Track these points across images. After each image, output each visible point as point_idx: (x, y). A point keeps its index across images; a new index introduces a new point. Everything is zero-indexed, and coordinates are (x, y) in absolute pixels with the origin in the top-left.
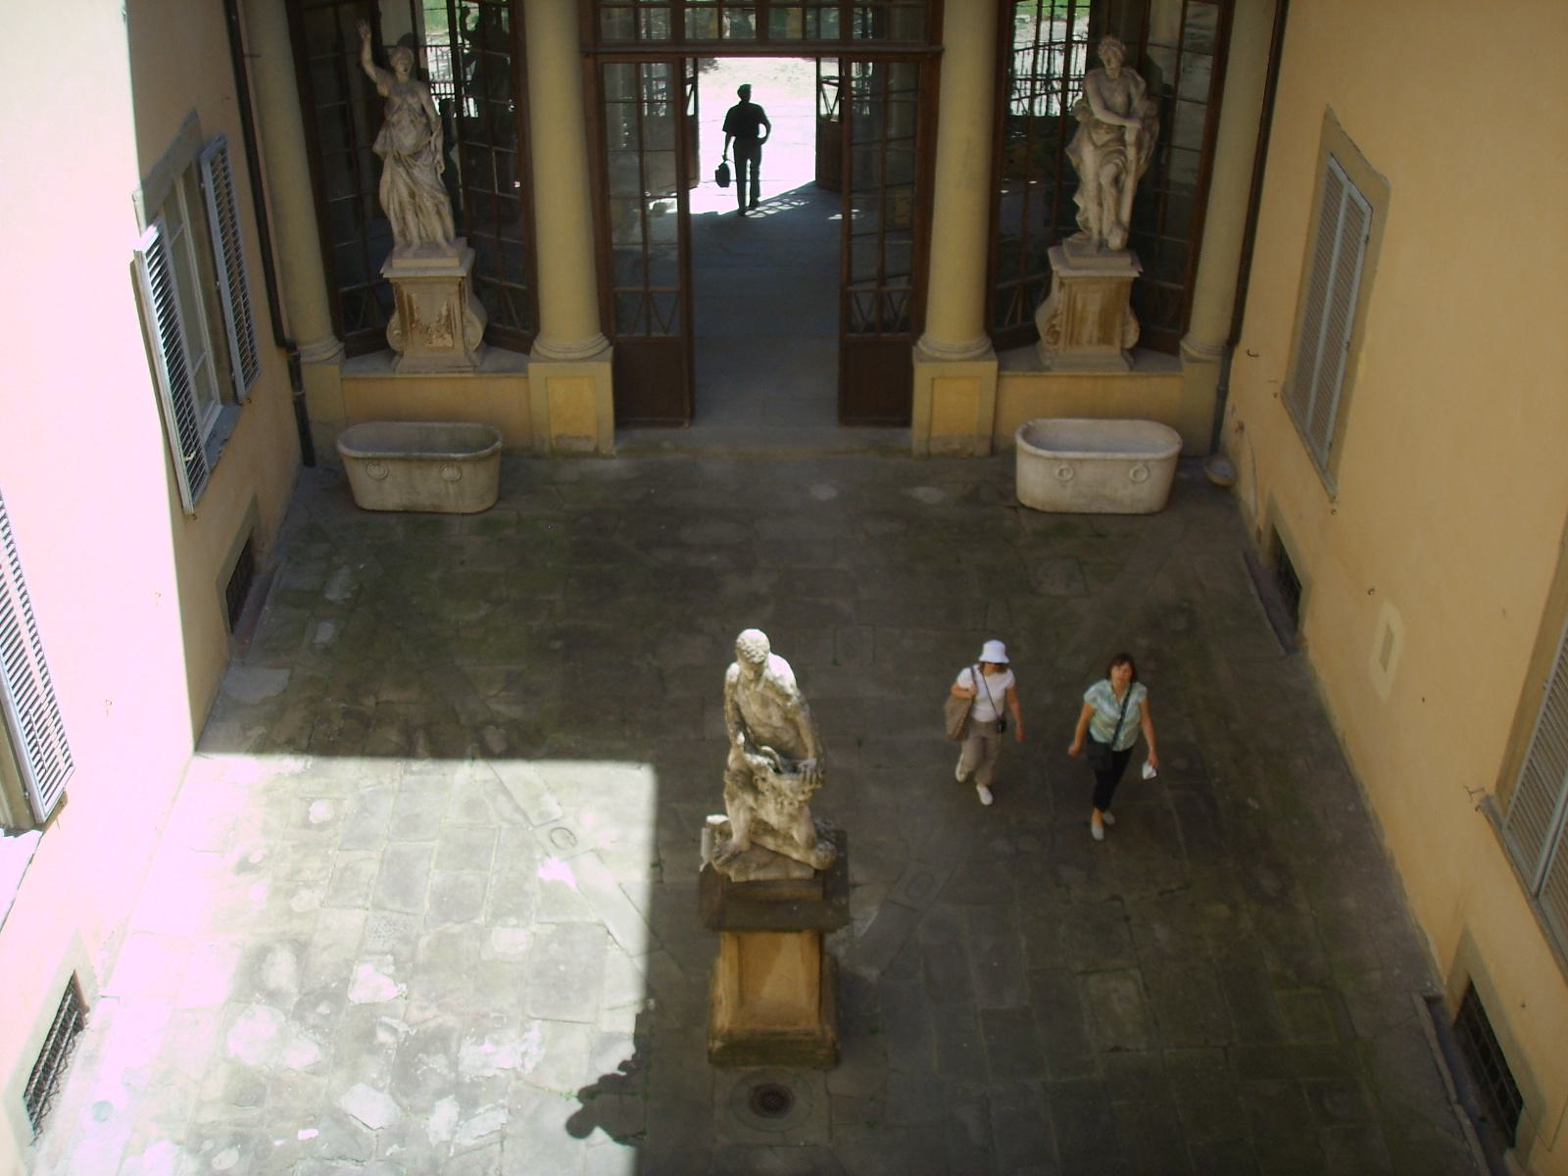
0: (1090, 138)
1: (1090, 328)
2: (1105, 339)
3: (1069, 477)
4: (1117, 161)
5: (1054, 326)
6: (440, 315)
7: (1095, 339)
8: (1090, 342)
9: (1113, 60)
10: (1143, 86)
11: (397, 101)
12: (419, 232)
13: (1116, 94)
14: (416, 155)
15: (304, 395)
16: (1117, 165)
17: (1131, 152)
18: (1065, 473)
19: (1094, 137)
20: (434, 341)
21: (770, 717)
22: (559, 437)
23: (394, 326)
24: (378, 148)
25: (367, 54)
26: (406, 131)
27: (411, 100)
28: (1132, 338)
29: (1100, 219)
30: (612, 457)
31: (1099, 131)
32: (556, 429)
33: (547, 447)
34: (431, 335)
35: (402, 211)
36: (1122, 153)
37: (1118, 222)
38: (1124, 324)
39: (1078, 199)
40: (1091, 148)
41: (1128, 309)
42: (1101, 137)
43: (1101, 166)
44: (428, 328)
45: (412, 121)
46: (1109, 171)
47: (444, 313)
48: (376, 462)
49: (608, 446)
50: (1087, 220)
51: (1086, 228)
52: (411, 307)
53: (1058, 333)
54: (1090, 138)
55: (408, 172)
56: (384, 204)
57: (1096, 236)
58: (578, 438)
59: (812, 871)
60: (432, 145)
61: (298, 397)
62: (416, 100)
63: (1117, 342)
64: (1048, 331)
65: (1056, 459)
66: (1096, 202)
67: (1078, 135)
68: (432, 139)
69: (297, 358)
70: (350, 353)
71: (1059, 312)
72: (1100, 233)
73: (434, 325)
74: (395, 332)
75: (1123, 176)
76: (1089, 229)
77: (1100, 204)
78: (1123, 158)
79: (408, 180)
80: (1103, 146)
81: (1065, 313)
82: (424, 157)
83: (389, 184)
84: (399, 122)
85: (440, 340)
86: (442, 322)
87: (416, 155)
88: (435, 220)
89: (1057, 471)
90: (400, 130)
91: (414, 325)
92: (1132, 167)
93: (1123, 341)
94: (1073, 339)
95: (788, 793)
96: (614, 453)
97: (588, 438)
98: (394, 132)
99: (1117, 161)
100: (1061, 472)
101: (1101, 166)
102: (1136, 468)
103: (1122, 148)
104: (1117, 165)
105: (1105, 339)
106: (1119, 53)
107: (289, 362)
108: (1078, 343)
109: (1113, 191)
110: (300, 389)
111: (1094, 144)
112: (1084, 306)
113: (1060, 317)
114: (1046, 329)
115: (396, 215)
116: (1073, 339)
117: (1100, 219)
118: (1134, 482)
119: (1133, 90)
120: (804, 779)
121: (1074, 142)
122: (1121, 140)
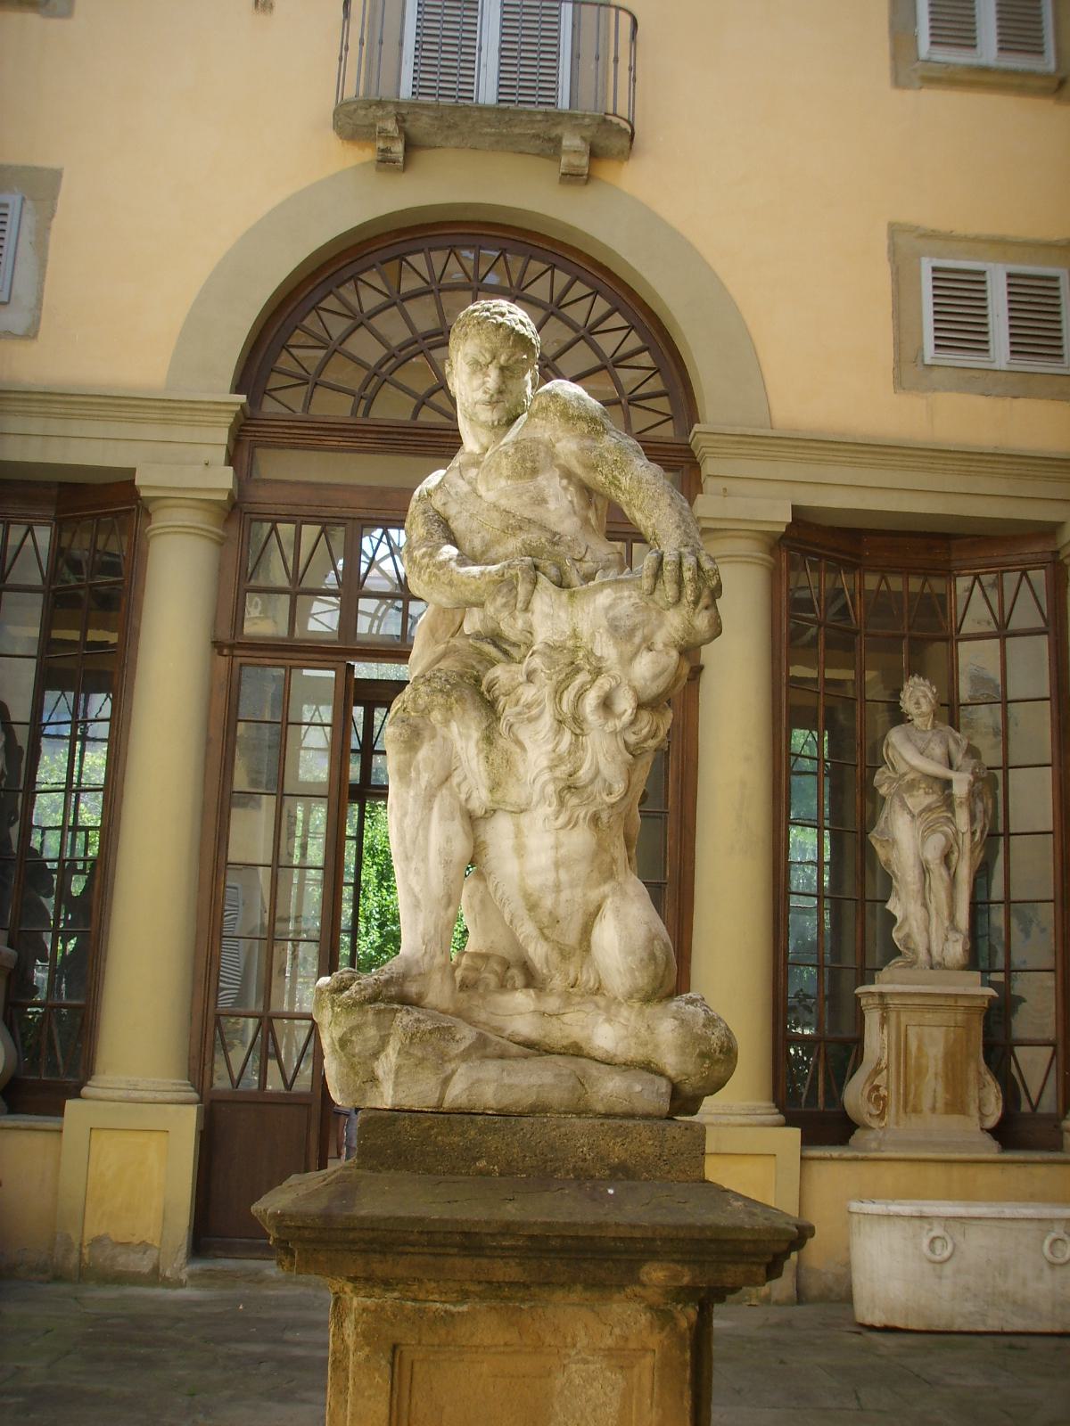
0: (904, 805)
1: (932, 1087)
2: (956, 1105)
3: (946, 1254)
4: (946, 828)
5: (877, 1088)
7: (940, 1105)
8: (933, 1109)
9: (922, 701)
13: (932, 745)
16: (946, 835)
17: (962, 818)
18: (938, 1244)
19: (909, 802)
21: (541, 501)
22: (98, 1241)
28: (994, 1112)
30: (180, 1284)
31: (915, 793)
32: (93, 1229)
33: (74, 1258)
36: (950, 821)
37: (954, 927)
38: (981, 1086)
39: (893, 906)
40: (908, 817)
41: (983, 1067)
42: (921, 799)
43: (924, 839)
46: (933, 852)
49: (176, 1262)
50: (908, 936)
51: (908, 949)
53: (884, 1098)
54: (904, 805)
57: (923, 956)
58: (126, 1244)
59: (664, 1086)
64: (869, 1098)
65: (921, 1217)
66: (919, 903)
67: (887, 807)
71: (883, 1065)
72: (929, 951)
75: (954, 857)
76: (914, 952)
77: (925, 906)
78: (952, 827)
81: (893, 1069)
89: (926, 1242)
94: (910, 1106)
95: (607, 649)
96: (184, 1277)
97: (145, 1246)
101: (924, 839)
102: (1053, 1235)
103: (950, 815)
105: (956, 1105)
106: (930, 695)
108: (916, 1110)
109: (944, 872)
111: (910, 812)
112: (920, 1048)
113: (885, 1072)
114: (866, 1093)
116: (910, 1106)
118: (1052, 1265)
119: (953, 746)
120: (658, 573)
121: (881, 824)
122: (948, 802)
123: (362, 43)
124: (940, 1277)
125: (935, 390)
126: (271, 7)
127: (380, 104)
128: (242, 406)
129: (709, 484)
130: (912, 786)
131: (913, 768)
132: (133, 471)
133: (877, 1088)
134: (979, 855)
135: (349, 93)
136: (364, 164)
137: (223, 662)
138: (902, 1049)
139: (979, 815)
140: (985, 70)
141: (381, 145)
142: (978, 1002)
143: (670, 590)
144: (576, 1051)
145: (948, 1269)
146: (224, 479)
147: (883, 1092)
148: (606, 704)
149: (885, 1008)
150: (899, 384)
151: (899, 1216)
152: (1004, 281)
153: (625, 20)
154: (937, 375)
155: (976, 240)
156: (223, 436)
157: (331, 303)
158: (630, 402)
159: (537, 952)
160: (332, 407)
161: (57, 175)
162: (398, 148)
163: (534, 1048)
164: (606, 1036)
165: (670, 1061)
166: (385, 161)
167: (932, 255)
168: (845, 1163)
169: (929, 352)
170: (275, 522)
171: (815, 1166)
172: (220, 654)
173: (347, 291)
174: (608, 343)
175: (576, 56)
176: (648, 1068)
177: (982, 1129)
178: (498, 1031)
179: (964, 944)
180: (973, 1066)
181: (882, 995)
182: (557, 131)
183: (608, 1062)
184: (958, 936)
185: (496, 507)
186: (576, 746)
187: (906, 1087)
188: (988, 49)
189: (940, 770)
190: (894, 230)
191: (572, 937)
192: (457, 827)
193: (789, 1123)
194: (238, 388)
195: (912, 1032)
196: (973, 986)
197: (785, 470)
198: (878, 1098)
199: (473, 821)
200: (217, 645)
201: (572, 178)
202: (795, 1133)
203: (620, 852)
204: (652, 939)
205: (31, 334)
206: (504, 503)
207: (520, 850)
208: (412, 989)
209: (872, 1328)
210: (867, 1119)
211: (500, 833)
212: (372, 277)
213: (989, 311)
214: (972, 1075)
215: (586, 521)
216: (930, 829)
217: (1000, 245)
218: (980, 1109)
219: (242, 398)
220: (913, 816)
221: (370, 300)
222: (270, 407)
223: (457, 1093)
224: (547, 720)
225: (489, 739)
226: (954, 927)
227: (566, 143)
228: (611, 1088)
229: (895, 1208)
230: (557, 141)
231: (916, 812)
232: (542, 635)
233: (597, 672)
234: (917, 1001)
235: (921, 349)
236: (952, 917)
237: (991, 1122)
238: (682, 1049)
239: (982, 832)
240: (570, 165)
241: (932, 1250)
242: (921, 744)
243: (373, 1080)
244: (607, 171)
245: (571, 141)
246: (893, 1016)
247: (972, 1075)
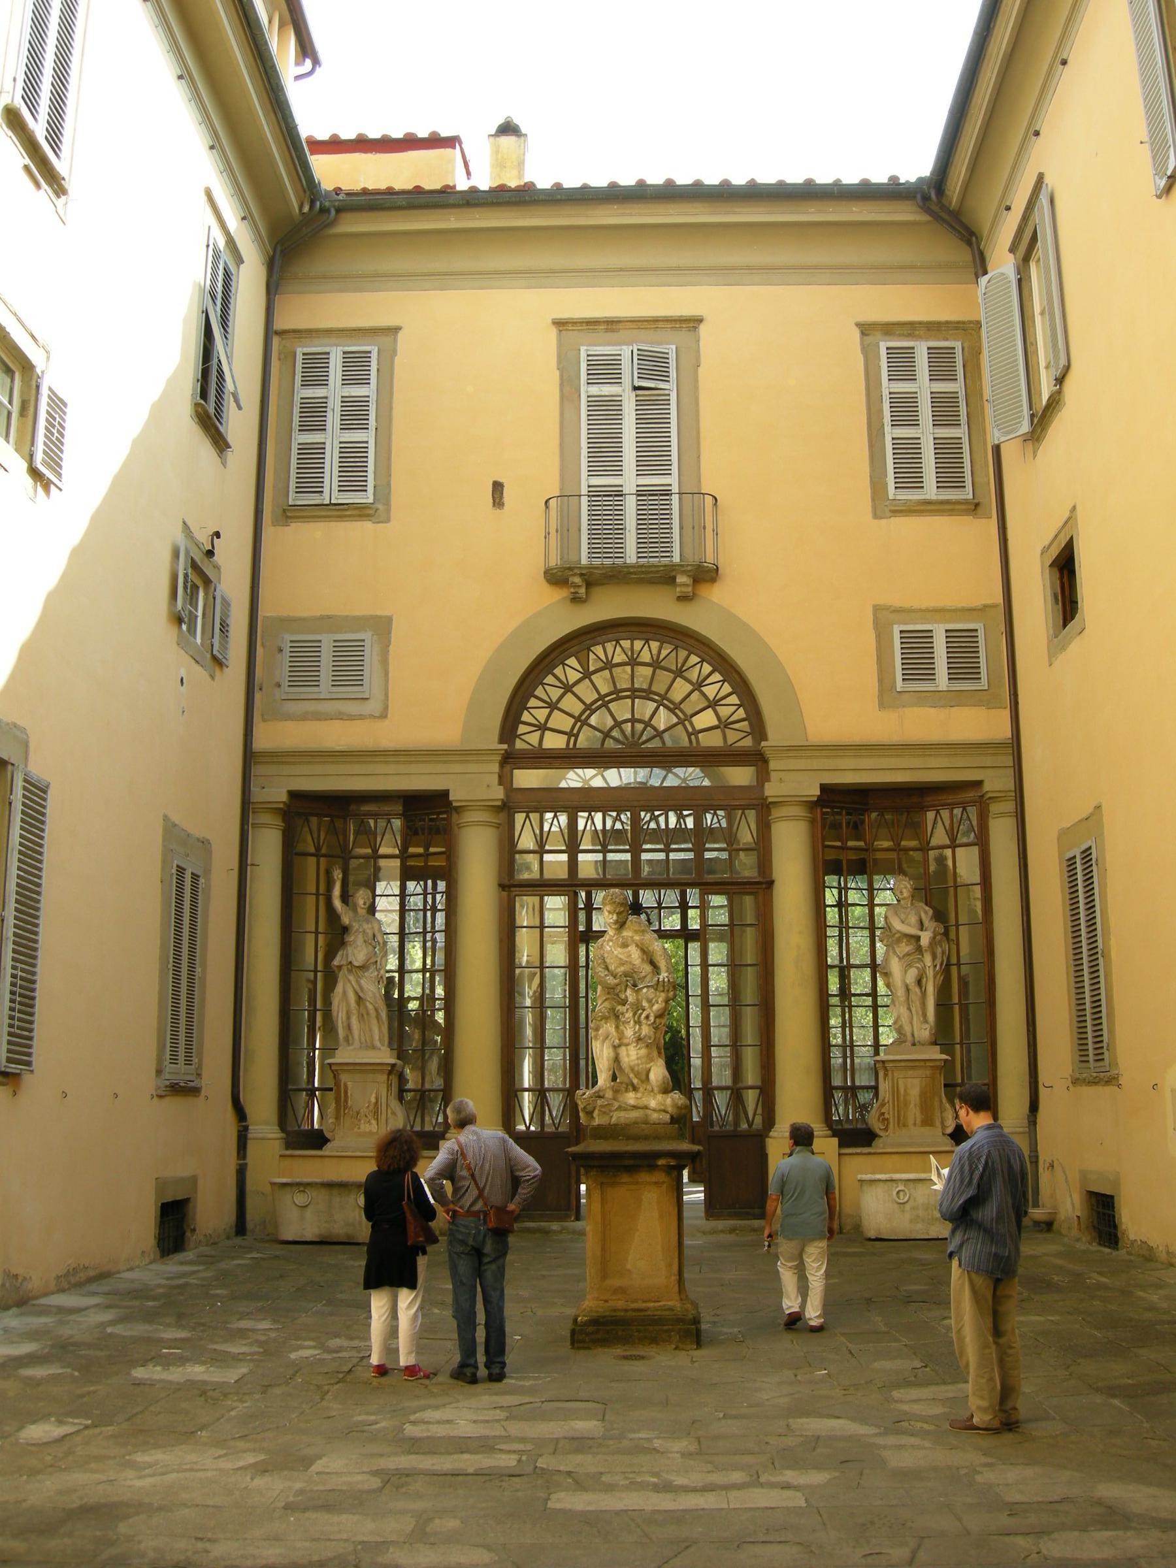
0: (895, 952)
1: (914, 1113)
2: (927, 1121)
4: (918, 965)
5: (883, 1114)
6: (369, 1102)
7: (918, 1121)
8: (915, 1124)
9: (904, 890)
10: (931, 912)
11: (356, 925)
12: (360, 1035)
14: (363, 968)
15: (246, 1164)
16: (918, 968)
18: (901, 1194)
20: (362, 1127)
23: (330, 1115)
24: (336, 962)
25: (337, 891)
26: (359, 948)
27: (366, 926)
29: (911, 1023)
34: (360, 1120)
35: (348, 1018)
36: (921, 960)
40: (897, 959)
41: (944, 1100)
42: (905, 948)
44: (358, 1113)
45: (365, 941)
47: (373, 1100)
48: (302, 1189)
52: (346, 1092)
53: (887, 1119)
54: (895, 952)
56: (334, 1014)
57: (909, 1038)
61: (240, 1165)
62: (370, 926)
63: (938, 1123)
65: (892, 1180)
69: (246, 1128)
70: (288, 1146)
72: (913, 1035)
73: (363, 1111)
74: (331, 1121)
75: (924, 980)
76: (905, 1035)
77: (909, 1009)
79: (356, 987)
80: (904, 956)
83: (341, 995)
84: (354, 941)
85: (367, 1125)
86: (371, 1108)
87: (363, 968)
88: (374, 1021)
89: (895, 1193)
92: (930, 973)
93: (944, 1127)
94: (902, 1123)
98: (350, 949)
99: (918, 965)
100: (898, 1193)
101: (906, 972)
104: (918, 968)
105: (927, 1121)
107: (239, 1131)
109: (917, 990)
110: (244, 1157)
111: (898, 956)
112: (905, 1090)
116: (902, 1123)
117: (911, 1023)
119: (923, 916)
122: (919, 949)
123: (557, 531)
124: (903, 1211)
125: (904, 707)
126: (503, 504)
127: (570, 569)
128: (506, 750)
129: (773, 775)
130: (899, 941)
131: (898, 932)
132: (445, 794)
133: (883, 1114)
134: (940, 979)
135: (553, 563)
136: (564, 598)
137: (505, 894)
138: (895, 1091)
139: (939, 955)
140: (929, 502)
141: (572, 590)
142: (938, 1064)
143: (662, 989)
144: (646, 1107)
145: (908, 1207)
146: (498, 793)
147: (886, 1116)
148: (647, 1017)
149: (886, 1069)
150: (882, 705)
151: (880, 1180)
152: (944, 634)
153: (709, 499)
154: (905, 697)
155: (927, 610)
156: (495, 768)
157: (550, 679)
158: (725, 727)
159: (635, 1081)
160: (553, 742)
161: (389, 620)
162: (582, 591)
163: (635, 1107)
164: (653, 1104)
165: (670, 1109)
166: (576, 600)
167: (899, 623)
168: (864, 1157)
169: (899, 684)
170: (528, 813)
171: (846, 1158)
172: (503, 890)
173: (558, 671)
174: (710, 691)
175: (681, 528)
176: (665, 1111)
177: (944, 1134)
178: (625, 1103)
179: (931, 1030)
180: (937, 1099)
181: (883, 1062)
182: (674, 574)
183: (654, 1110)
184: (927, 1026)
185: (617, 956)
186: (640, 1029)
187: (899, 1111)
188: (931, 490)
189: (913, 931)
190: (877, 609)
191: (644, 1077)
192: (611, 1050)
193: (834, 1136)
194: (501, 741)
195: (901, 1082)
196: (935, 1054)
197: (815, 764)
198: (884, 1120)
199: (615, 1047)
200: (502, 887)
201: (684, 598)
202: (835, 1141)
203: (655, 1053)
204: (664, 1078)
205: (384, 715)
206: (620, 956)
207: (628, 1055)
208: (601, 1094)
209: (870, 1240)
210: (878, 1131)
211: (623, 1051)
212: (572, 661)
213: (935, 655)
214: (936, 1104)
215: (643, 960)
216: (909, 966)
217: (940, 613)
218: (942, 1123)
219: (505, 746)
220: (900, 958)
221: (573, 676)
222: (519, 745)
223: (614, 1120)
224: (632, 1022)
225: (617, 1027)
226: (926, 1021)
227: (678, 580)
228: (655, 1116)
229: (879, 1176)
230: (674, 579)
231: (901, 956)
232: (630, 999)
233: (644, 1010)
234: (903, 1064)
235: (895, 682)
236: (925, 1015)
237: (950, 1130)
238: (672, 1106)
239: (941, 965)
240: (681, 592)
241: (899, 1198)
242: (903, 916)
243: (593, 1117)
244: (704, 590)
245: (681, 579)
246: (890, 1073)
247: (936, 1104)
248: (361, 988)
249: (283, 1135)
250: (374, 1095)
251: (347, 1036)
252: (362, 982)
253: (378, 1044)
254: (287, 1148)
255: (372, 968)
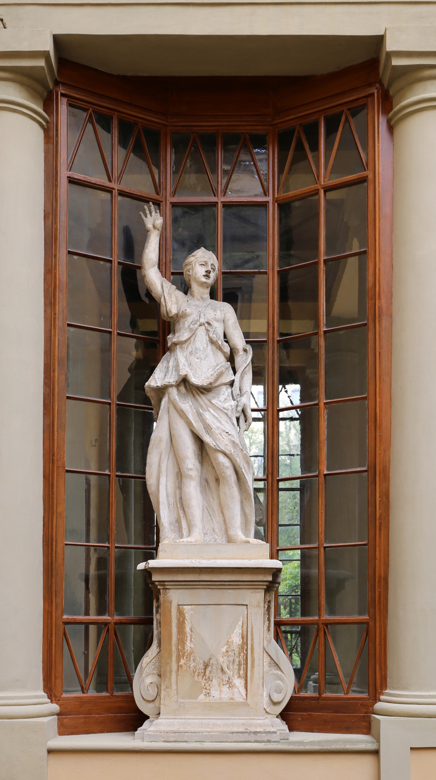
20: (215, 693)
23: (147, 670)
34: (209, 679)
44: (206, 666)
47: (237, 640)
55: (200, 415)
60: (236, 384)
68: (237, 378)
74: (148, 680)
82: (222, 398)
85: (225, 689)
88: (235, 491)
90: (191, 353)
91: (182, 662)
115: (167, 496)
248: (208, 428)
249: (55, 707)
250: (238, 630)
251: (178, 521)
252: (207, 416)
253: (240, 535)
254: (61, 733)
255: (226, 391)
